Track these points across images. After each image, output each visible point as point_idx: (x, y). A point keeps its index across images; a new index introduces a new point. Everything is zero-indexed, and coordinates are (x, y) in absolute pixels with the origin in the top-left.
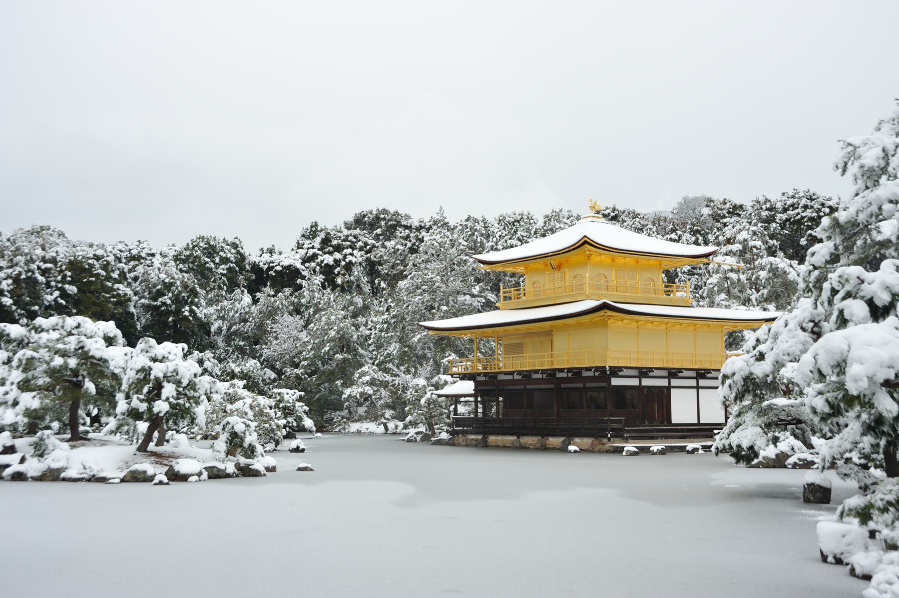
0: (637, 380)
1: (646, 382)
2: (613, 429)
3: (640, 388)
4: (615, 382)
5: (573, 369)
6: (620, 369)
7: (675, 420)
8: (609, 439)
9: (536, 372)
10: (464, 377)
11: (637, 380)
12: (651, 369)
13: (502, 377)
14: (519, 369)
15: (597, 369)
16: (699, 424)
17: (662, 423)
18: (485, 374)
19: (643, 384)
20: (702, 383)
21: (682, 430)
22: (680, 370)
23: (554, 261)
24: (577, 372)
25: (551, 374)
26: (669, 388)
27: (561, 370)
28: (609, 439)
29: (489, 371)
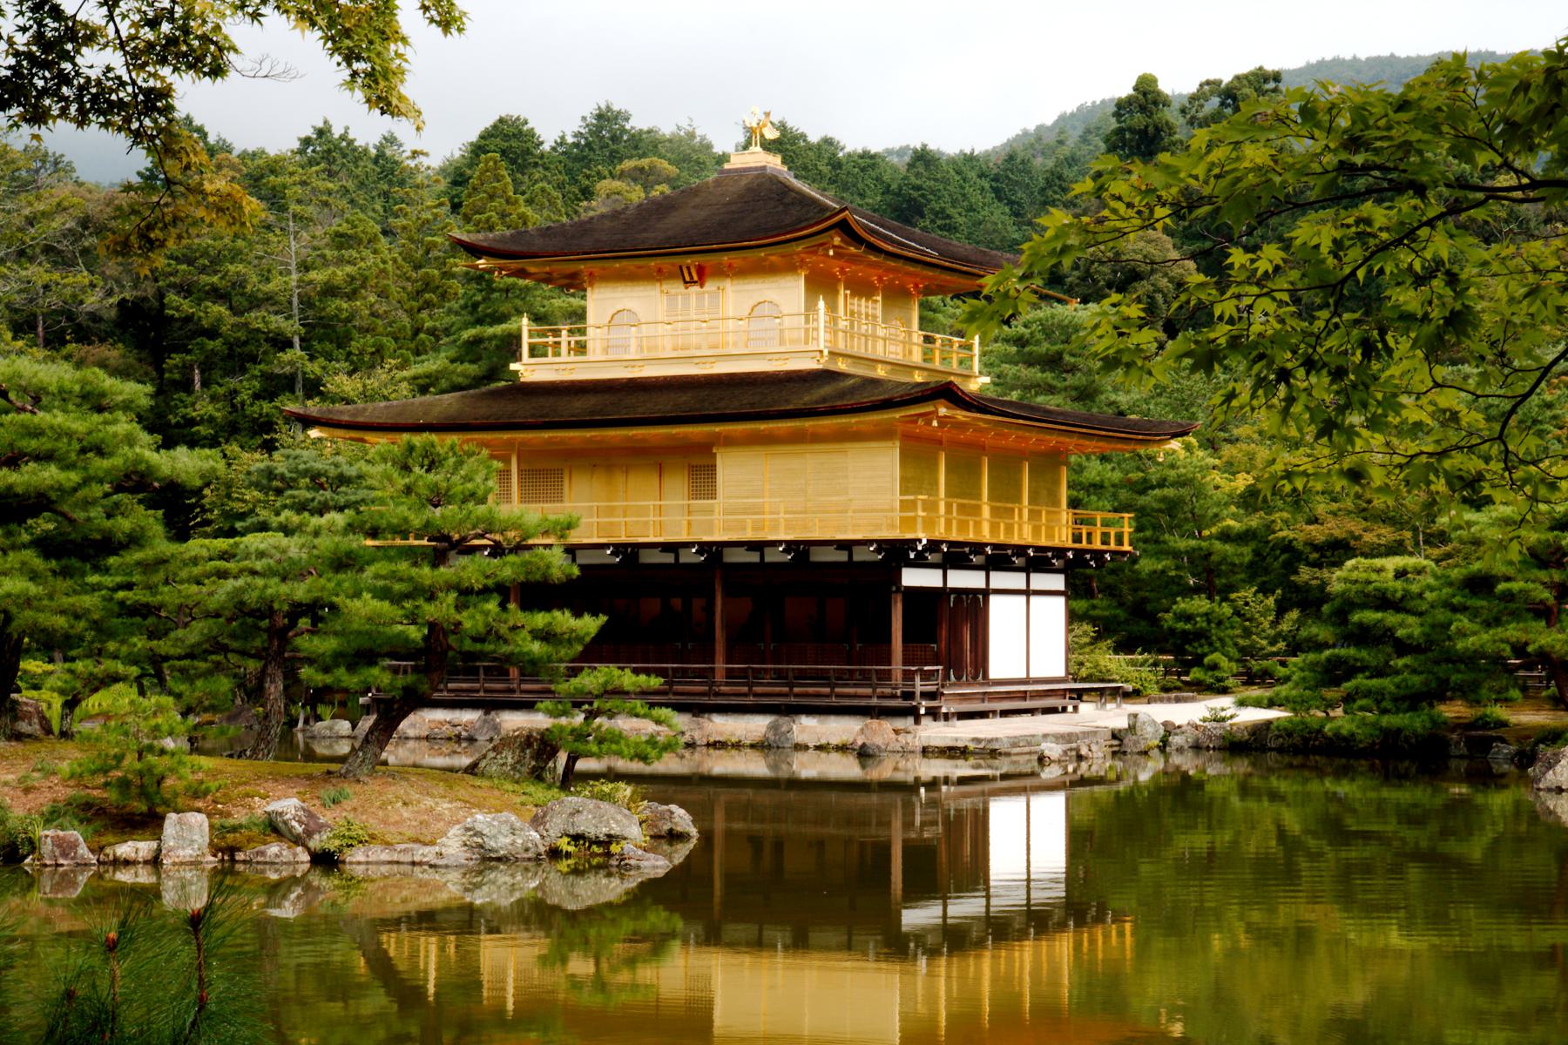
0: (940, 572)
2: (924, 695)
3: (942, 593)
4: (913, 578)
7: (994, 674)
8: (917, 722)
11: (940, 572)
12: (978, 547)
14: (623, 539)
15: (882, 545)
19: (949, 585)
20: (1040, 581)
21: (1024, 696)
24: (800, 548)
26: (986, 592)
28: (917, 722)
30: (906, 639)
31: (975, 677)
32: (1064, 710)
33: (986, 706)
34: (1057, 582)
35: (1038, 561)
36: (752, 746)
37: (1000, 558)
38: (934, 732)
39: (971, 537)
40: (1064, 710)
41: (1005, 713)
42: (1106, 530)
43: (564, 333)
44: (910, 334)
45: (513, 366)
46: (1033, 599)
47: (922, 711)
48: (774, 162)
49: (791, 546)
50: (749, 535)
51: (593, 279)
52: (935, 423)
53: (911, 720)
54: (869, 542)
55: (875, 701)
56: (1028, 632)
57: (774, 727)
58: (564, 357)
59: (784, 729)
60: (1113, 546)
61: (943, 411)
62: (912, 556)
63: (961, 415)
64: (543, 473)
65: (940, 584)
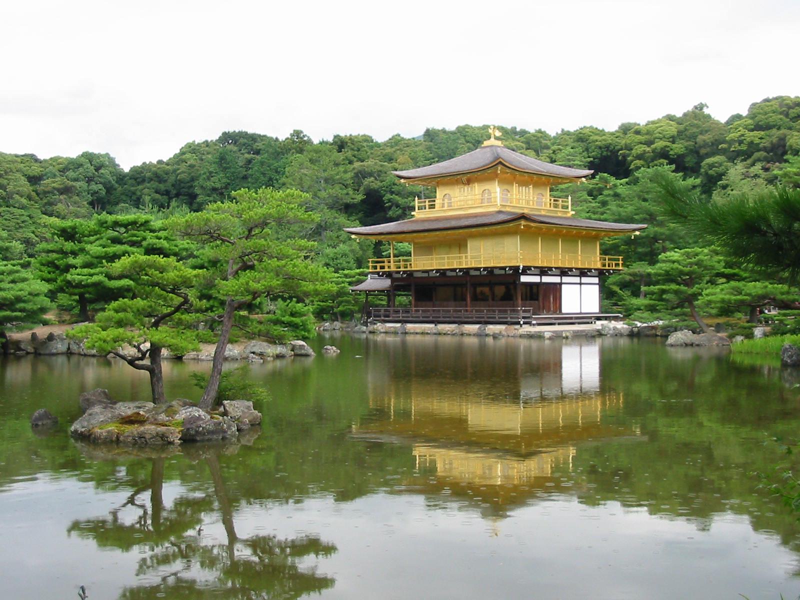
0: (539, 277)
1: (546, 279)
4: (524, 279)
5: (488, 268)
6: (529, 268)
7: (563, 311)
8: (521, 326)
9: (454, 270)
10: (380, 275)
12: (550, 269)
13: (416, 275)
15: (511, 268)
16: (581, 313)
17: (555, 313)
18: (404, 272)
20: (584, 280)
21: (571, 318)
22: (571, 269)
23: (464, 178)
24: (490, 270)
25: (466, 271)
26: (561, 284)
27: (478, 269)
28: (521, 326)
29: (409, 269)
30: (522, 300)
31: (558, 312)
32: (592, 323)
33: (553, 321)
34: (596, 280)
35: (583, 273)
36: (474, 335)
37: (564, 272)
38: (526, 329)
39: (587, 266)
40: (592, 323)
41: (559, 324)
42: (609, 262)
43: (427, 202)
44: (546, 199)
45: (413, 213)
46: (582, 286)
47: (522, 323)
48: (499, 143)
49: (485, 269)
50: (473, 266)
51: (438, 184)
52: (522, 227)
53: (519, 326)
54: (507, 267)
55: (509, 319)
56: (581, 298)
57: (479, 328)
58: (427, 210)
59: (483, 329)
60: (614, 268)
61: (523, 222)
62: (520, 271)
63: (532, 224)
64: (427, 248)
65: (539, 281)
